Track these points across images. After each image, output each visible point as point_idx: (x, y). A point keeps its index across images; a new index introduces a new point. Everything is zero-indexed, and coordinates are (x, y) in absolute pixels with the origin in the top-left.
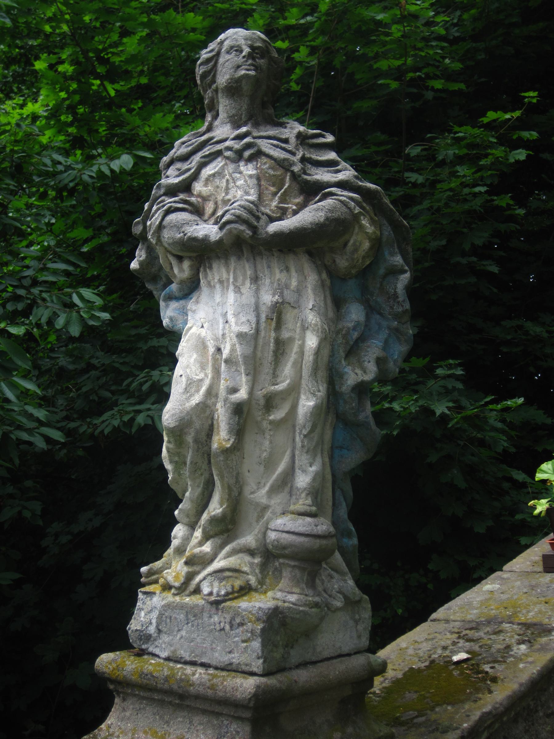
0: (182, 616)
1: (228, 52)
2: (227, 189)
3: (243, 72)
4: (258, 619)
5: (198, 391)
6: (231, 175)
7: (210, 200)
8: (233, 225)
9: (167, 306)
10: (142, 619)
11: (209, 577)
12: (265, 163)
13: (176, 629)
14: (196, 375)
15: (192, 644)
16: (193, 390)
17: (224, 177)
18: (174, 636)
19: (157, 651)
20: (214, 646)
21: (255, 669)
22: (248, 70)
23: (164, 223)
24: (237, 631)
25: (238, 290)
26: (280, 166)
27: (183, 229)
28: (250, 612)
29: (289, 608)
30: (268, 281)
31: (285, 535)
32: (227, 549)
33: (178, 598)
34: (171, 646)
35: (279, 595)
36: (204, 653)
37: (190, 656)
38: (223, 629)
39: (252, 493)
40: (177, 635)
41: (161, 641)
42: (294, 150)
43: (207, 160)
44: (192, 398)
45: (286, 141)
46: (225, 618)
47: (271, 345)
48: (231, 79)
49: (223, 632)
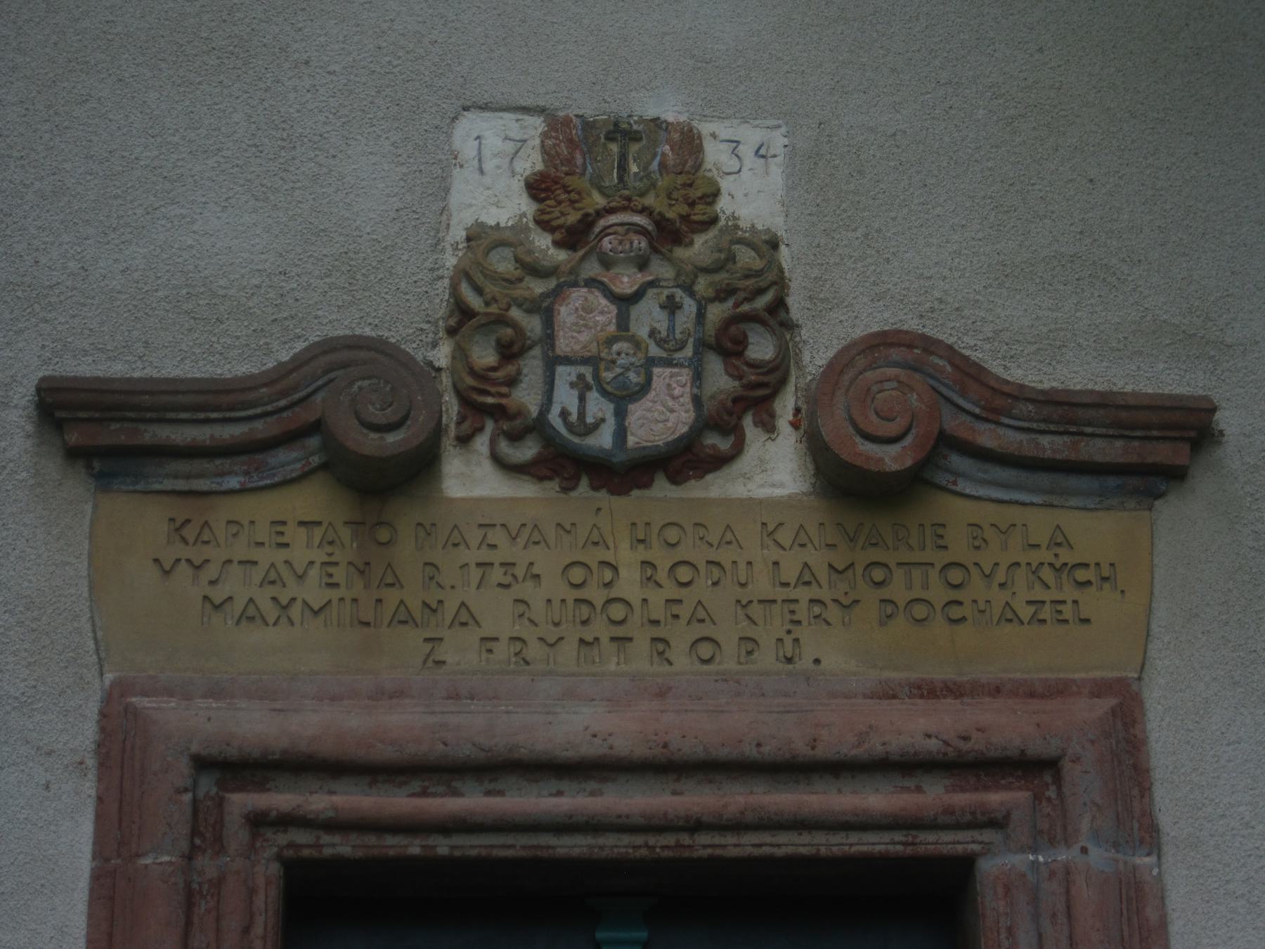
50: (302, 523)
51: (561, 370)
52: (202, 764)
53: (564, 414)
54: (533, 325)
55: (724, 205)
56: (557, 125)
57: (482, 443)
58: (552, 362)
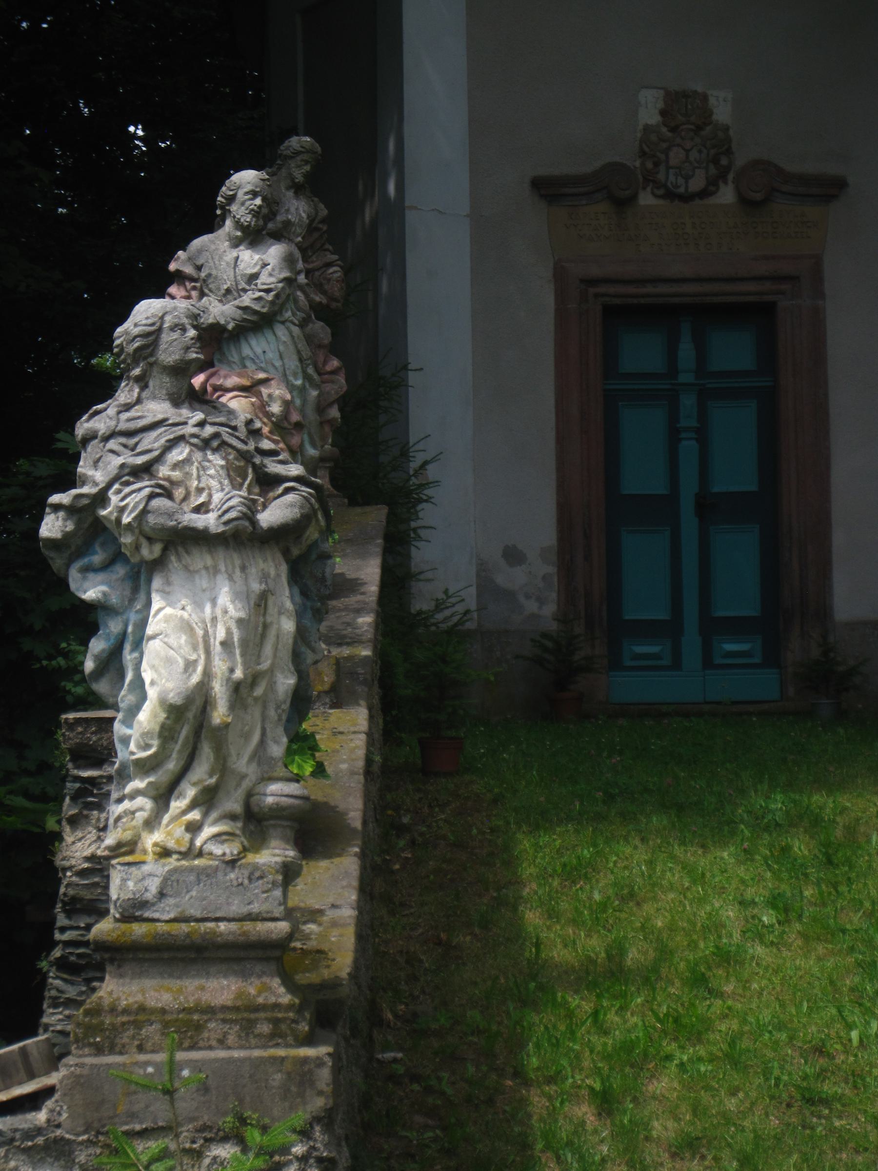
0: (192, 878)
1: (172, 329)
2: (199, 478)
3: (194, 355)
4: (277, 872)
5: (195, 671)
6: (200, 463)
7: (180, 486)
8: (240, 522)
9: (85, 578)
10: (131, 888)
11: (209, 842)
12: (230, 454)
13: (185, 890)
14: (190, 655)
15: (204, 902)
16: (191, 670)
17: (192, 464)
18: (182, 898)
19: (156, 915)
20: (230, 900)
21: (277, 915)
22: (197, 353)
23: (149, 508)
24: (257, 884)
25: (231, 578)
26: (242, 457)
27: (175, 517)
28: (269, 866)
29: (292, 862)
30: (254, 570)
31: (284, 799)
32: (214, 815)
33: (184, 863)
34: (178, 907)
35: (277, 851)
36: (218, 909)
37: (202, 913)
38: (242, 884)
39: (235, 763)
40: (185, 897)
41: (162, 905)
42: (246, 439)
43: (171, 443)
44: (191, 678)
45: (235, 428)
46: (243, 874)
47: (260, 629)
48: (181, 360)
49: (241, 887)
50: (603, 213)
51: (671, 171)
52: (582, 281)
53: (672, 183)
54: (662, 157)
55: (715, 117)
56: (668, 94)
57: (649, 189)
58: (668, 168)
